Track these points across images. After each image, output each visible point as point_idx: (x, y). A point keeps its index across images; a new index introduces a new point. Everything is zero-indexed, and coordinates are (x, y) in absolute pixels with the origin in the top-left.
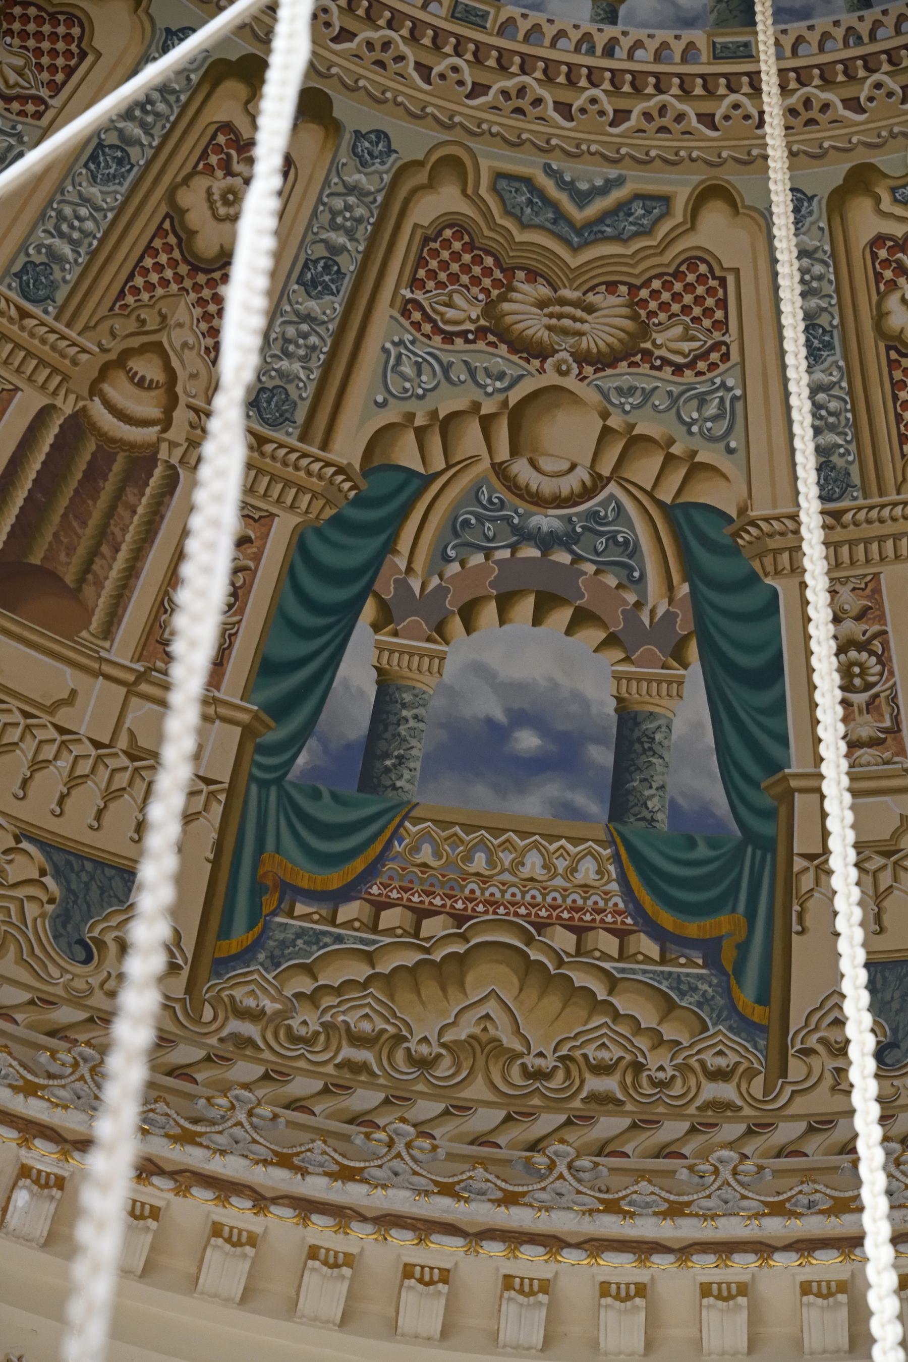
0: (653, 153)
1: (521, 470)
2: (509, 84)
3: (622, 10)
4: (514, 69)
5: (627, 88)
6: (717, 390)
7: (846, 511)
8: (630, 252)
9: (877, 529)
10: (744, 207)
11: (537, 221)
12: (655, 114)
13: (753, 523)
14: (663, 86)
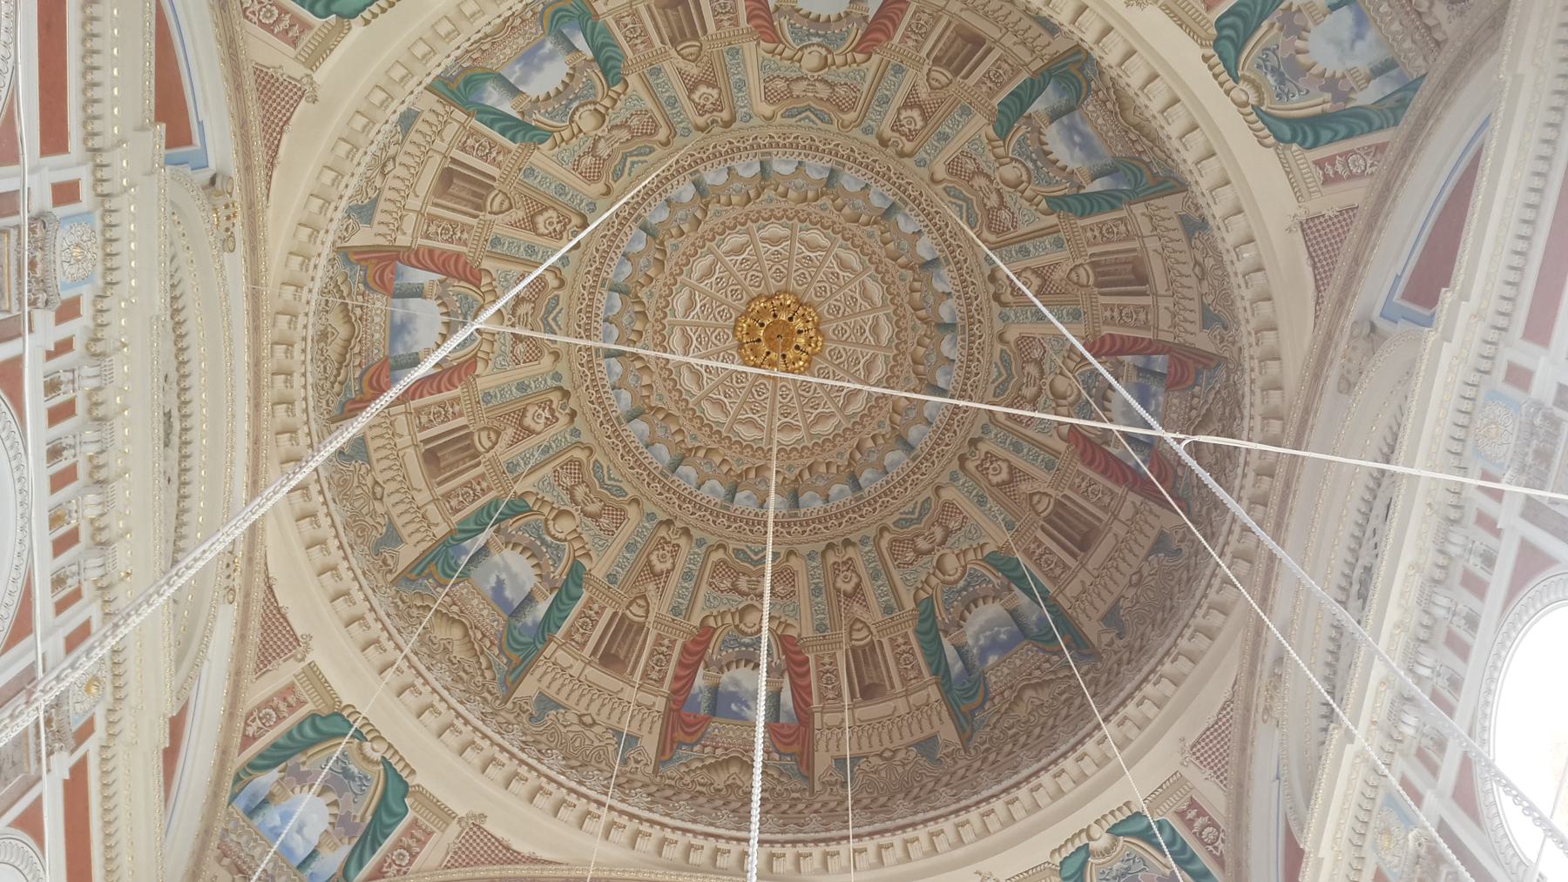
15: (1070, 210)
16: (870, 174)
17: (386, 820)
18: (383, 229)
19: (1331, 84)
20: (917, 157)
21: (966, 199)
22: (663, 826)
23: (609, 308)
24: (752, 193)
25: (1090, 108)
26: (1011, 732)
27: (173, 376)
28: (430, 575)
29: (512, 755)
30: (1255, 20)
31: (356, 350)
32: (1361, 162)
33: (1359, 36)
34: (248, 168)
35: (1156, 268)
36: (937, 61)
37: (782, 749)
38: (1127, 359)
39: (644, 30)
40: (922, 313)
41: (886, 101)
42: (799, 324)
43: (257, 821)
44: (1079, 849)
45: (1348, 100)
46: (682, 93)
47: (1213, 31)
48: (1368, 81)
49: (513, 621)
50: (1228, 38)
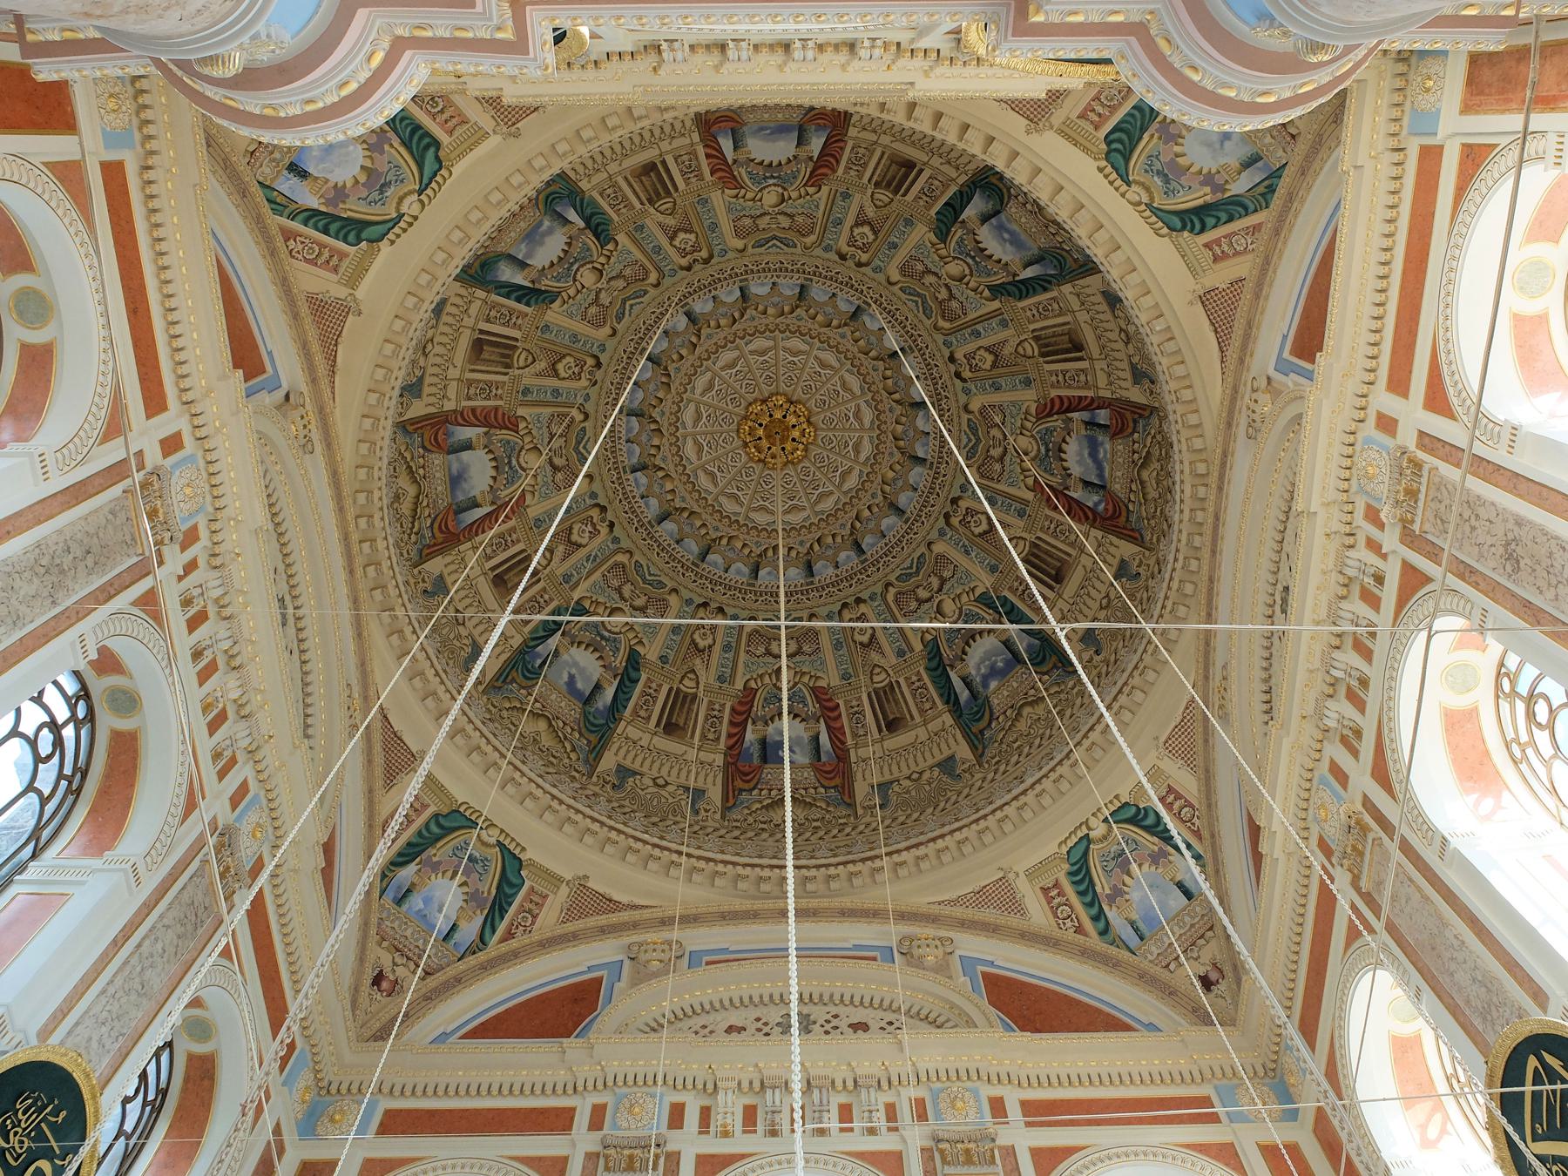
16: (835, 285)
17: (508, 891)
18: (432, 400)
19: (1208, 179)
20: (873, 265)
21: (919, 295)
22: (734, 864)
23: (629, 430)
24: (737, 315)
25: (1013, 210)
26: (1016, 745)
27: (281, 567)
28: (513, 680)
29: (602, 824)
30: (1138, 132)
31: (425, 504)
32: (1243, 241)
34: (314, 381)
35: (1089, 337)
36: (877, 185)
37: (826, 783)
38: (1075, 415)
39: (625, 196)
40: (896, 396)
41: (840, 222)
42: (792, 420)
43: (405, 907)
44: (1081, 839)
45: (1225, 190)
46: (664, 242)
47: (1104, 146)
49: (587, 708)
50: (1116, 150)
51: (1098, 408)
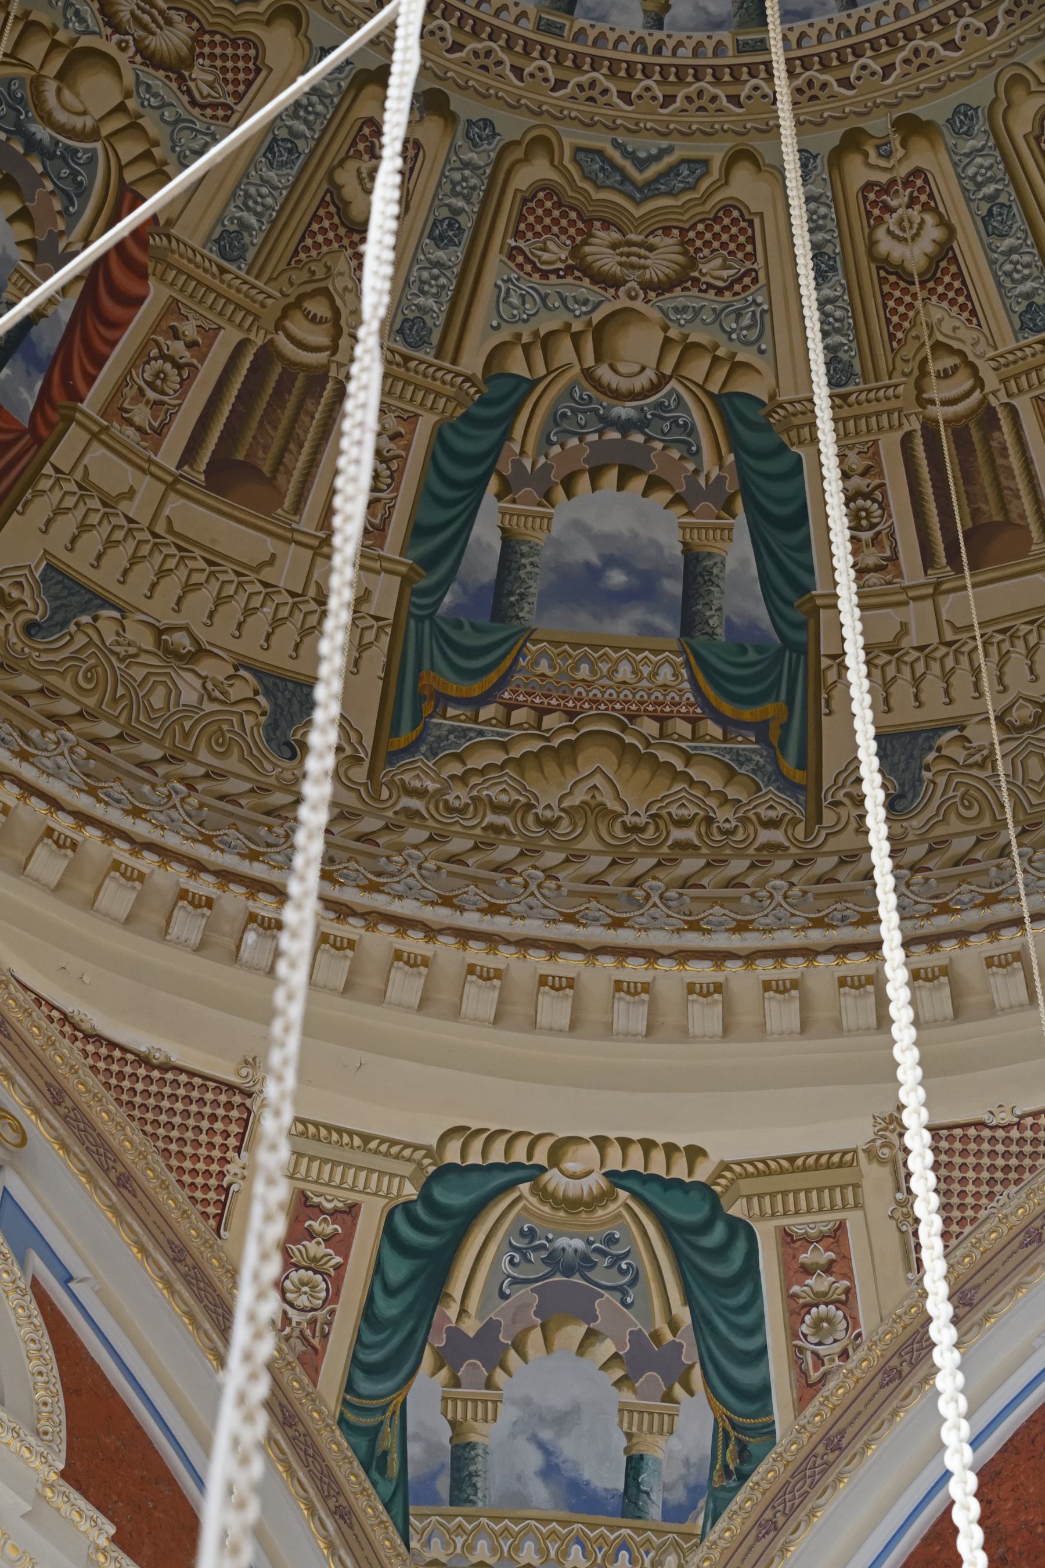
0: (694, 127)
1: (604, 373)
2: (584, 79)
3: (667, 19)
4: (586, 67)
5: (672, 78)
6: (749, 306)
7: (850, 394)
8: (680, 203)
9: (875, 407)
10: (765, 165)
11: (608, 182)
12: (695, 97)
13: (781, 406)
14: (699, 76)
15: (467, 418)
16: (870, 32)
21: (649, 190)
30: (705, 1303)
32: (303, 1301)
33: (550, 1471)
36: (987, 417)
45: (441, 1360)
47: (737, 1210)
48: (453, 1424)
50: (706, 1227)
51: (45, 394)
